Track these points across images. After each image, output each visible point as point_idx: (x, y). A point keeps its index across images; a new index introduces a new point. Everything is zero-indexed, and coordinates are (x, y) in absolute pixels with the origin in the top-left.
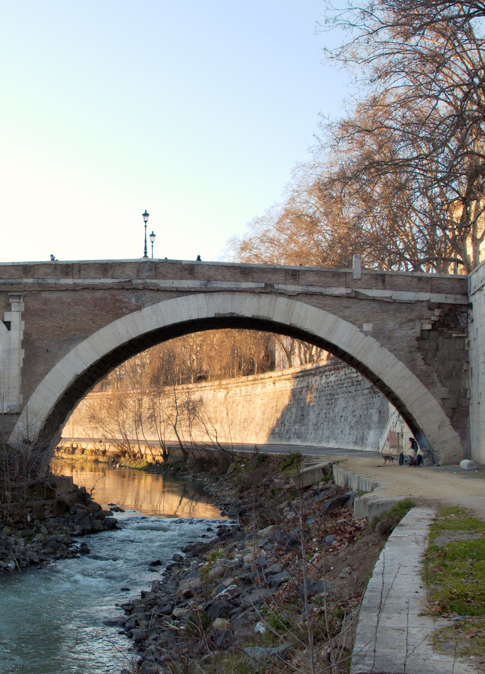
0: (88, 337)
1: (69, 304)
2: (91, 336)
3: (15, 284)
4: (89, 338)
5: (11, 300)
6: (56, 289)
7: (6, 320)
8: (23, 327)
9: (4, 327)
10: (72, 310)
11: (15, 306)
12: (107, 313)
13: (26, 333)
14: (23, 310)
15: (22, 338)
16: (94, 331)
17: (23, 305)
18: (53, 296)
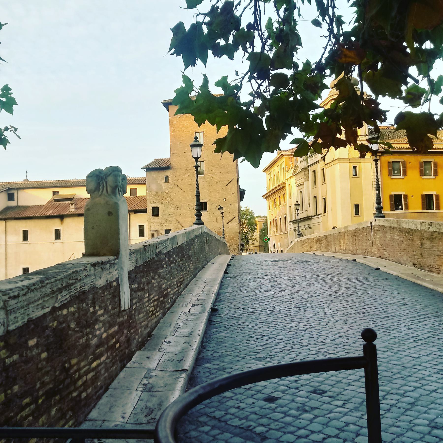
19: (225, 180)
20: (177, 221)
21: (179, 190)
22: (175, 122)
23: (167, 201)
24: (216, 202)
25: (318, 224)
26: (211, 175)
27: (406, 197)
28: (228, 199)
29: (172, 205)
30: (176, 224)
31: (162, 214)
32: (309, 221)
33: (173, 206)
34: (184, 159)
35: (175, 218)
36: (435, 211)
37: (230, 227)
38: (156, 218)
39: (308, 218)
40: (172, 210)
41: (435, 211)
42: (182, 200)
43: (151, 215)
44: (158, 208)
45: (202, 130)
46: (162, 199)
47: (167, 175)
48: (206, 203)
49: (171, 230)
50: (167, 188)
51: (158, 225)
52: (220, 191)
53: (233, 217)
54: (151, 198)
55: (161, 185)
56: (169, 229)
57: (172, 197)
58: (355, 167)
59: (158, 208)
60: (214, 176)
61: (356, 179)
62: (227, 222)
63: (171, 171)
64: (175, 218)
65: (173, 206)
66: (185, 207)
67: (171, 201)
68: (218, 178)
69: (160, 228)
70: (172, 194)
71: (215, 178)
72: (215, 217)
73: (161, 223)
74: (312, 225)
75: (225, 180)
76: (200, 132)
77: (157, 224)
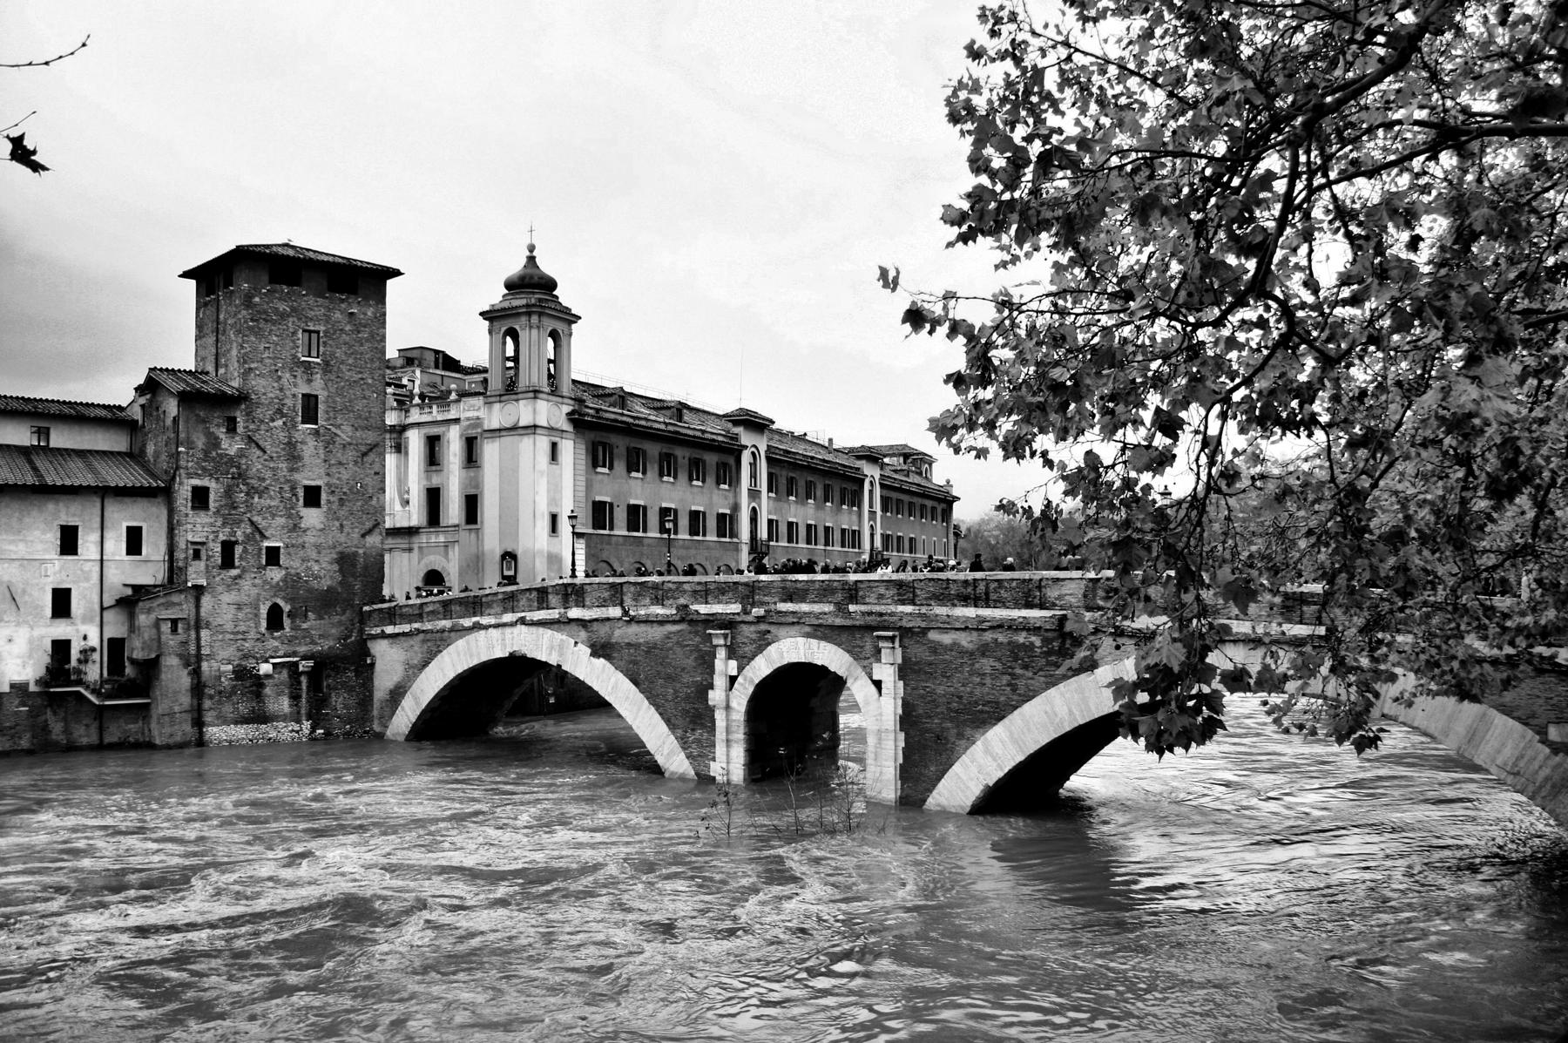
0: (1004, 717)
1: (972, 654)
2: (1010, 717)
3: (885, 614)
4: (1006, 721)
5: (881, 644)
6: (948, 626)
7: (875, 677)
8: (901, 692)
9: (873, 689)
10: (977, 666)
11: (886, 655)
12: (1035, 674)
13: (905, 704)
14: (900, 661)
15: (900, 711)
16: (1016, 708)
17: (899, 651)
18: (947, 639)
20: (252, 523)
21: (261, 454)
22: (257, 299)
26: (333, 429)
27: (611, 505)
36: (700, 538)
38: (202, 513)
39: (411, 532)
41: (640, 534)
43: (190, 504)
44: (206, 490)
45: (317, 328)
46: (217, 470)
49: (236, 542)
50: (231, 446)
54: (190, 464)
56: (233, 539)
58: (554, 446)
59: (206, 490)
60: (338, 432)
63: (243, 406)
69: (211, 537)
73: (212, 525)
76: (310, 332)
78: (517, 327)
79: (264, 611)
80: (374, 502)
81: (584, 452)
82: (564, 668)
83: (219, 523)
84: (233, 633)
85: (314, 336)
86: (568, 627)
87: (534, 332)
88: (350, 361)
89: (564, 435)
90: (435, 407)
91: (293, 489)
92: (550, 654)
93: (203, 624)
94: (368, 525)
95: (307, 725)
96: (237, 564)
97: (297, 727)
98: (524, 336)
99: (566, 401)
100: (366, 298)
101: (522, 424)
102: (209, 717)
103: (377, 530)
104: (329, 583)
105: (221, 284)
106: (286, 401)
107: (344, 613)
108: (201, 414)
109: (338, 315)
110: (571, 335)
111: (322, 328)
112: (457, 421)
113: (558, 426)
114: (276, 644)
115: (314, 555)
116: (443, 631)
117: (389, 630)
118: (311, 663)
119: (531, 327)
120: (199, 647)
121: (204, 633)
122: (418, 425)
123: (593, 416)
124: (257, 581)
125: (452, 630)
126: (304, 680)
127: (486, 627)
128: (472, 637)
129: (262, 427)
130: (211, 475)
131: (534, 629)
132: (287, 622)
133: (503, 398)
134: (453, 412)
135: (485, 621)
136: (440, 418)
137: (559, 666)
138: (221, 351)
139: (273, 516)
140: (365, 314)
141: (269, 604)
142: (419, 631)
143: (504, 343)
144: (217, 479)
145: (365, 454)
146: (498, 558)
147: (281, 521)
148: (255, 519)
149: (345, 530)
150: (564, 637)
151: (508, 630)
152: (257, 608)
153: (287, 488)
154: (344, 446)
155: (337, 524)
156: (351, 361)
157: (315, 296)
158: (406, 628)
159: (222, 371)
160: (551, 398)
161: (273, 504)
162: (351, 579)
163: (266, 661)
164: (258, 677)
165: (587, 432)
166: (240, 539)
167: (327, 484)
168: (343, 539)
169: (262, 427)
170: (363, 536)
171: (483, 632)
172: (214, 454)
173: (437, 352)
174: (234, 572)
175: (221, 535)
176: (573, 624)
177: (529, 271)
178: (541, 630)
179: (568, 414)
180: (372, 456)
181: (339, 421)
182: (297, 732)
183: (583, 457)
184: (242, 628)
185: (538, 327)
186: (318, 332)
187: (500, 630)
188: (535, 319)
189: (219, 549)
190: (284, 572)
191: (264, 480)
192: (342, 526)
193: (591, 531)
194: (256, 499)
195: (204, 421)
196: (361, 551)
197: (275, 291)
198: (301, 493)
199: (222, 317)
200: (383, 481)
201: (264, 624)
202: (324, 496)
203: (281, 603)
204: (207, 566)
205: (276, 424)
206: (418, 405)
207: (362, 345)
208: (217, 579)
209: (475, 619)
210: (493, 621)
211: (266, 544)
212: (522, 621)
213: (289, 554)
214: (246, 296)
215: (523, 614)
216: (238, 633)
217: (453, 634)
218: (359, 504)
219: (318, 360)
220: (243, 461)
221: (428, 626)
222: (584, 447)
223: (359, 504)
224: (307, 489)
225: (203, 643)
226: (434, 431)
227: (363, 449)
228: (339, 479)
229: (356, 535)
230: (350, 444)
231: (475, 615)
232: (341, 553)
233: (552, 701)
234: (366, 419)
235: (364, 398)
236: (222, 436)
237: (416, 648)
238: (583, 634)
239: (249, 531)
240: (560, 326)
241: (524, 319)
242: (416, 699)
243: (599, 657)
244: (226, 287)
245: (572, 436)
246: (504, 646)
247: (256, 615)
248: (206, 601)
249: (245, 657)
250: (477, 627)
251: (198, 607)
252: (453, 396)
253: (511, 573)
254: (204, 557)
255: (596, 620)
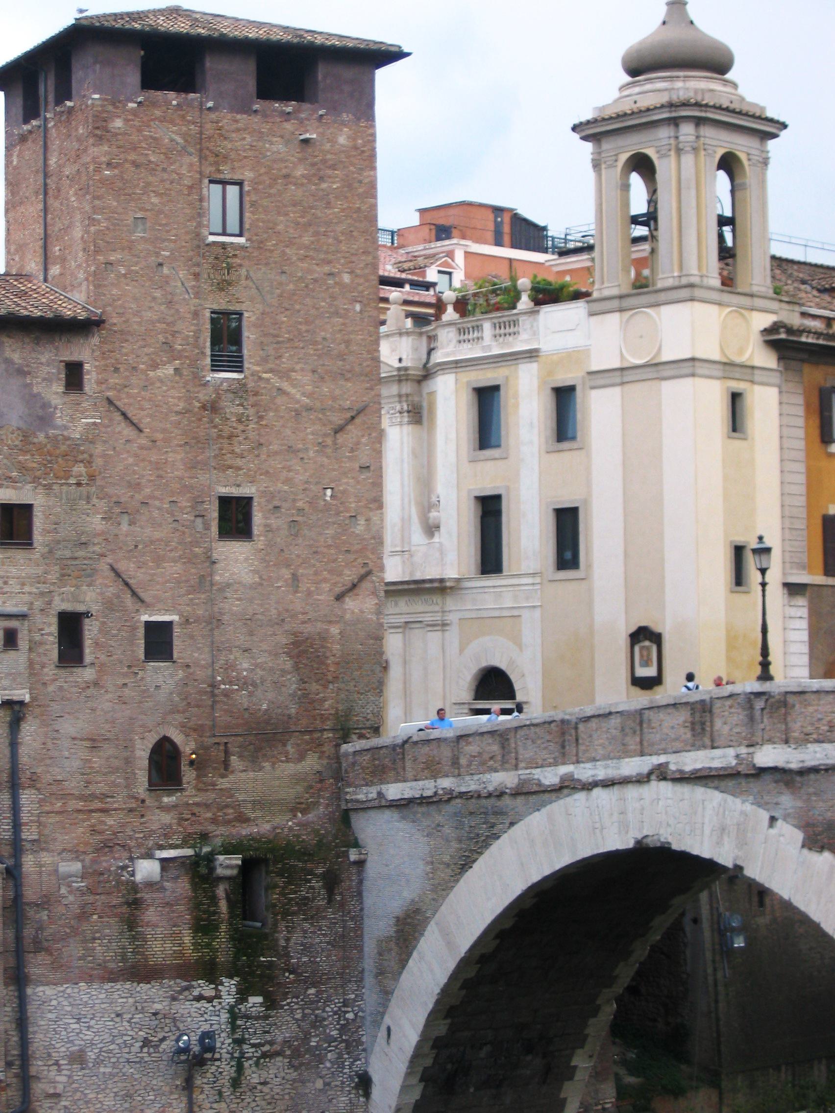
19: (332, 409)
20: (118, 574)
21: (128, 432)
22: (118, 123)
23: (72, 481)
24: (294, 501)
25: (515, 613)
26: (276, 381)
28: (344, 492)
29: (95, 501)
30: (113, 589)
31: (49, 538)
32: (437, 598)
33: (102, 505)
34: (158, 294)
35: (109, 560)
37: (348, 616)
40: (96, 523)
42: (144, 481)
45: (237, 177)
47: (75, 358)
48: (250, 499)
49: (87, 614)
51: (27, 589)
52: (311, 454)
53: (363, 571)
55: (45, 405)
56: (81, 608)
57: (99, 462)
58: (735, 398)
60: (285, 386)
61: (737, 444)
62: (338, 590)
63: (95, 340)
64: (109, 560)
65: (102, 505)
66: (156, 513)
67: (92, 477)
68: (303, 394)
69: (38, 604)
70: (99, 449)
71: (287, 394)
72: (288, 566)
74: (453, 618)
75: (332, 409)
77: (23, 584)
78: (651, 152)
79: (142, 753)
80: (360, 527)
81: (800, 411)
82: (749, 872)
83: (53, 577)
84: (82, 798)
85: (233, 191)
86: (755, 786)
87: (688, 160)
88: (307, 239)
89: (758, 376)
90: (487, 326)
91: (197, 502)
92: (719, 843)
93: (24, 779)
94: (349, 576)
95: (229, 987)
96: (88, 658)
97: (209, 991)
98: (664, 168)
99: (758, 302)
100: (334, 108)
101: (666, 357)
102: (37, 965)
103: (366, 585)
104: (270, 695)
105: (51, 98)
106: (180, 326)
107: (301, 757)
108: (16, 357)
109: (278, 147)
110: (765, 162)
111: (248, 175)
112: (532, 355)
113: (743, 359)
114: (167, 818)
115: (242, 639)
116: (500, 794)
117: (394, 791)
118: (236, 860)
119: (679, 151)
120: (17, 825)
121: (27, 798)
122: (457, 365)
123: (818, 334)
124: (127, 691)
125: (517, 793)
126: (221, 891)
127: (589, 786)
128: (558, 807)
129: (134, 380)
130: (35, 480)
131: (685, 790)
132: (188, 775)
133: (627, 302)
134: (524, 336)
135: (585, 772)
136: (496, 351)
137: (739, 868)
138: (54, 230)
139: (159, 560)
140: (333, 141)
141: (152, 739)
142: (451, 796)
143: (626, 187)
144: (48, 487)
145: (339, 430)
146: (623, 641)
147: (174, 569)
148: (121, 566)
149: (303, 587)
150: (748, 807)
151: (632, 792)
152: (129, 746)
153: (184, 502)
154: (298, 413)
155: (286, 573)
156: (307, 239)
157: (233, 109)
158: (427, 787)
159: (55, 270)
160: (726, 298)
161: (157, 535)
162: (314, 687)
163: (149, 856)
164: (134, 887)
165: (807, 369)
166: (94, 609)
167: (263, 493)
168: (298, 606)
169: (134, 380)
170: (339, 597)
171: (581, 796)
172: (41, 437)
173: (498, 210)
174: (88, 674)
175: (57, 600)
176: (767, 777)
177: (676, 34)
178: (699, 792)
179: (766, 331)
180: (353, 432)
181: (286, 363)
182: (210, 1000)
183: (801, 422)
184: (100, 788)
185: (695, 150)
186: (240, 184)
187: (615, 791)
188: (687, 130)
189: (54, 629)
190: (181, 675)
191: (137, 486)
192: (295, 577)
193: (819, 579)
194: (125, 527)
195: (21, 372)
196: (335, 630)
197: (154, 104)
198: (214, 514)
199: (53, 161)
200: (378, 484)
201: (142, 777)
202: (258, 518)
203: (177, 738)
204: (31, 664)
205: (159, 373)
206: (450, 324)
207: (328, 205)
208: (51, 688)
209: (564, 770)
210: (601, 772)
211: (145, 618)
212: (661, 773)
213: (192, 637)
214: (96, 117)
215: (662, 759)
216: (93, 797)
217: (520, 800)
218: (330, 532)
219: (241, 240)
220: (99, 449)
221: (470, 784)
222: (800, 400)
223: (330, 532)
224: (225, 502)
225: (25, 817)
226: (486, 377)
227: (337, 419)
228: (287, 481)
229: (324, 597)
230: (309, 409)
231: (562, 758)
232: (295, 634)
233: (739, 943)
234: (341, 356)
235: (337, 314)
236: (56, 401)
237: (447, 830)
238: (787, 801)
239: (111, 591)
240: (741, 145)
241: (664, 133)
242: (446, 934)
243: (822, 849)
244: (59, 101)
245: (776, 378)
246: (624, 826)
247: (128, 761)
248: (29, 730)
249: (106, 847)
250: (568, 786)
251: (14, 745)
252: (525, 302)
253: (650, 672)
254: (23, 643)
255: (815, 770)
